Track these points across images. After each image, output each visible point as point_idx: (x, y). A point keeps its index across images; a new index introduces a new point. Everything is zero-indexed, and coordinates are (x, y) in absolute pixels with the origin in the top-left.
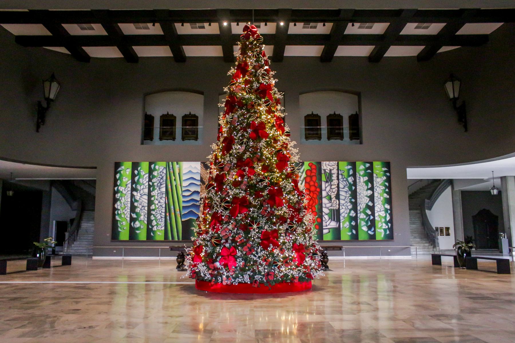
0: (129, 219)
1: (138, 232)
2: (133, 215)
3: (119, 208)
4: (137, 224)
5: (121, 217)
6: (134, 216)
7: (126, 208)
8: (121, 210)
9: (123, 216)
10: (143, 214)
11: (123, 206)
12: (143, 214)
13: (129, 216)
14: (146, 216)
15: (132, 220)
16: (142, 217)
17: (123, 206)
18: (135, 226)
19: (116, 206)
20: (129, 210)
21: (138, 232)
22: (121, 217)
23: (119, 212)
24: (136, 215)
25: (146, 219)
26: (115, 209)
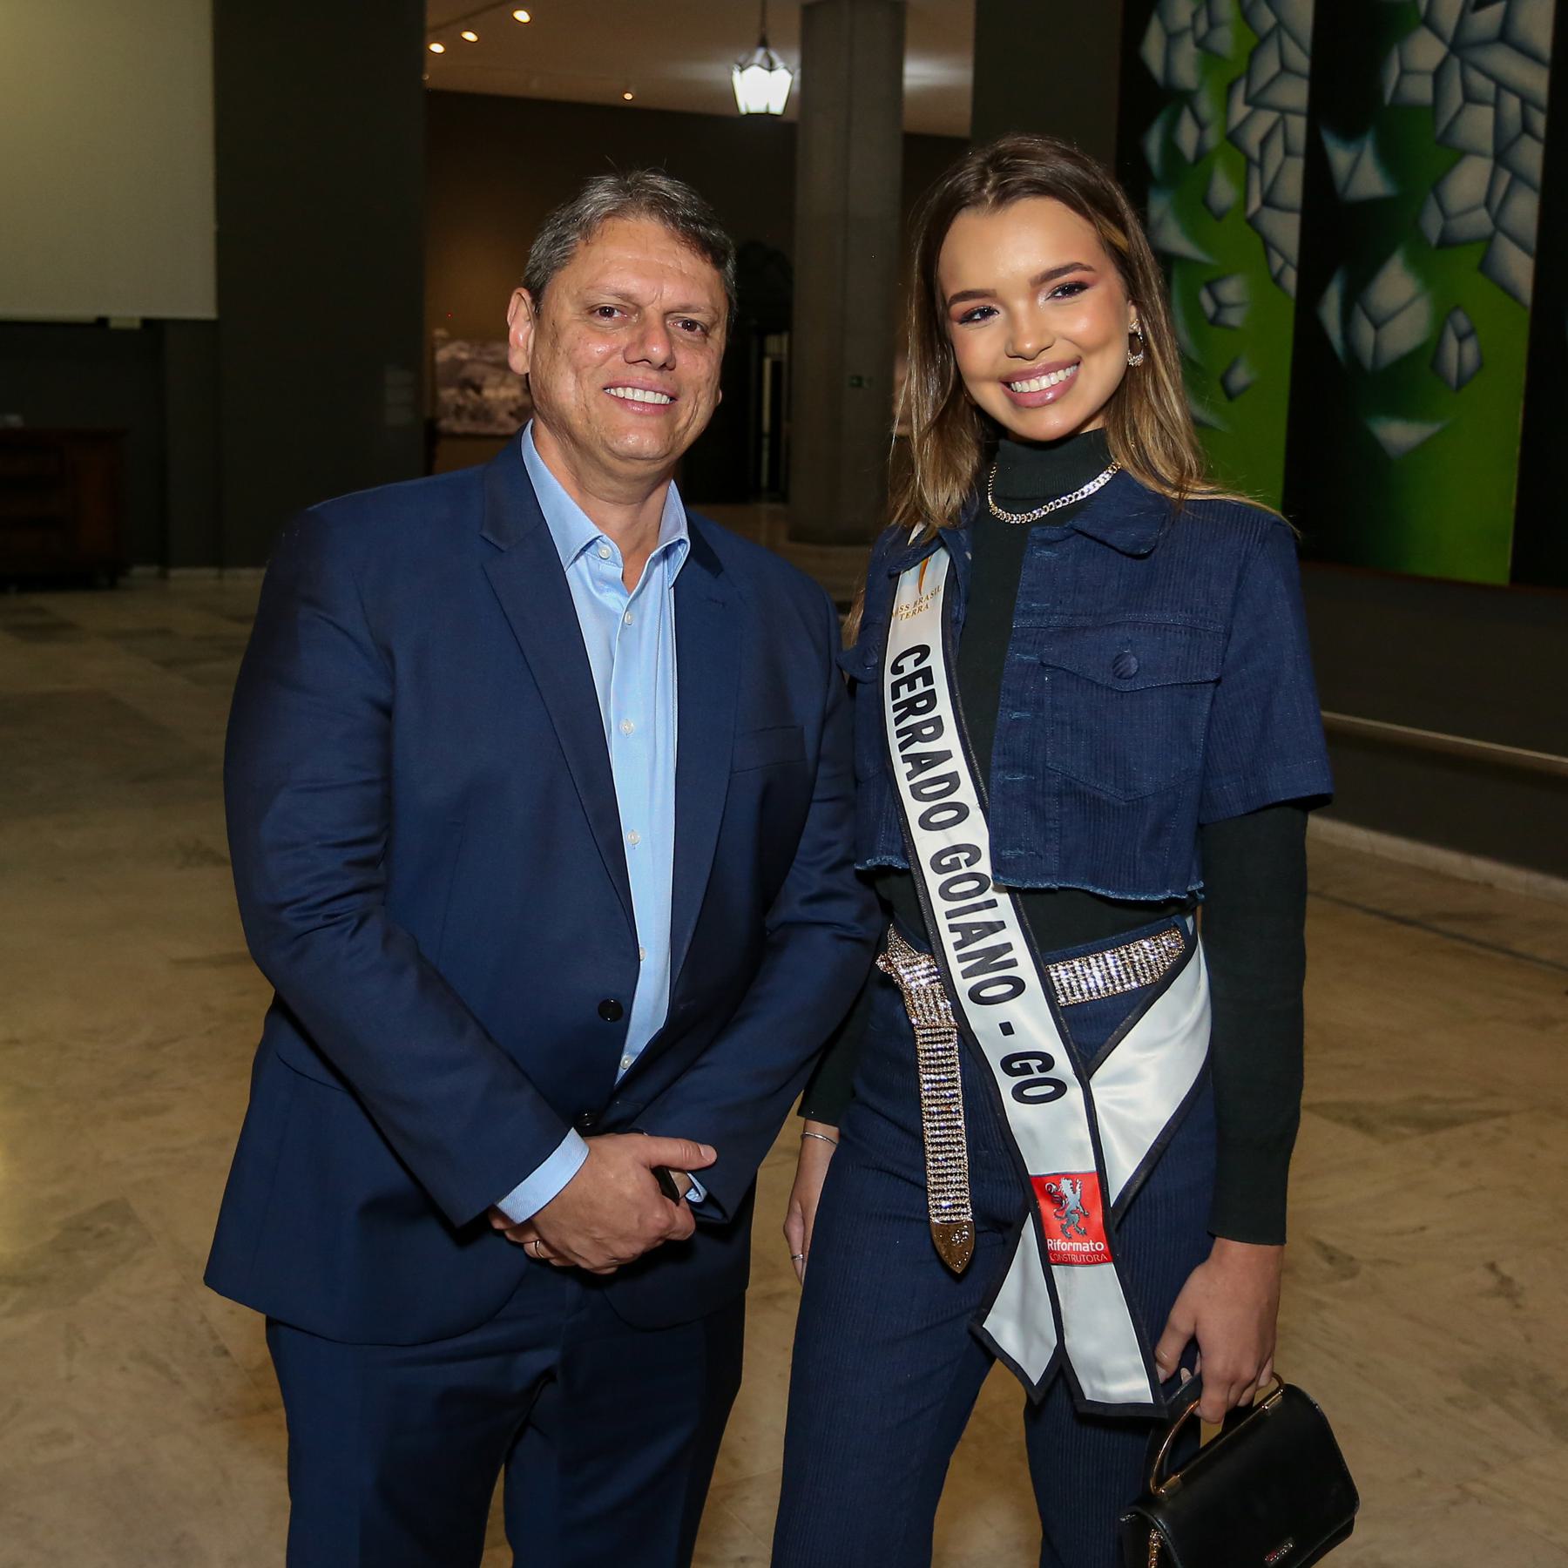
0: (1286, 230)
1: (1397, 434)
2: (1340, 157)
3: (1186, 71)
4: (1400, 307)
5: (1199, 211)
6: (1362, 173)
7: (1269, 65)
8: (1206, 107)
9: (1223, 191)
10: (1478, 125)
11: (1226, 40)
12: (1478, 125)
13: (1292, 188)
14: (1531, 155)
15: (1342, 241)
16: (1469, 182)
17: (1226, 40)
18: (1365, 334)
19: (1153, 50)
20: (1295, 93)
21: (1397, 434)
22: (1199, 211)
23: (1187, 136)
24: (1389, 159)
25: (1525, 209)
26: (1146, 98)
